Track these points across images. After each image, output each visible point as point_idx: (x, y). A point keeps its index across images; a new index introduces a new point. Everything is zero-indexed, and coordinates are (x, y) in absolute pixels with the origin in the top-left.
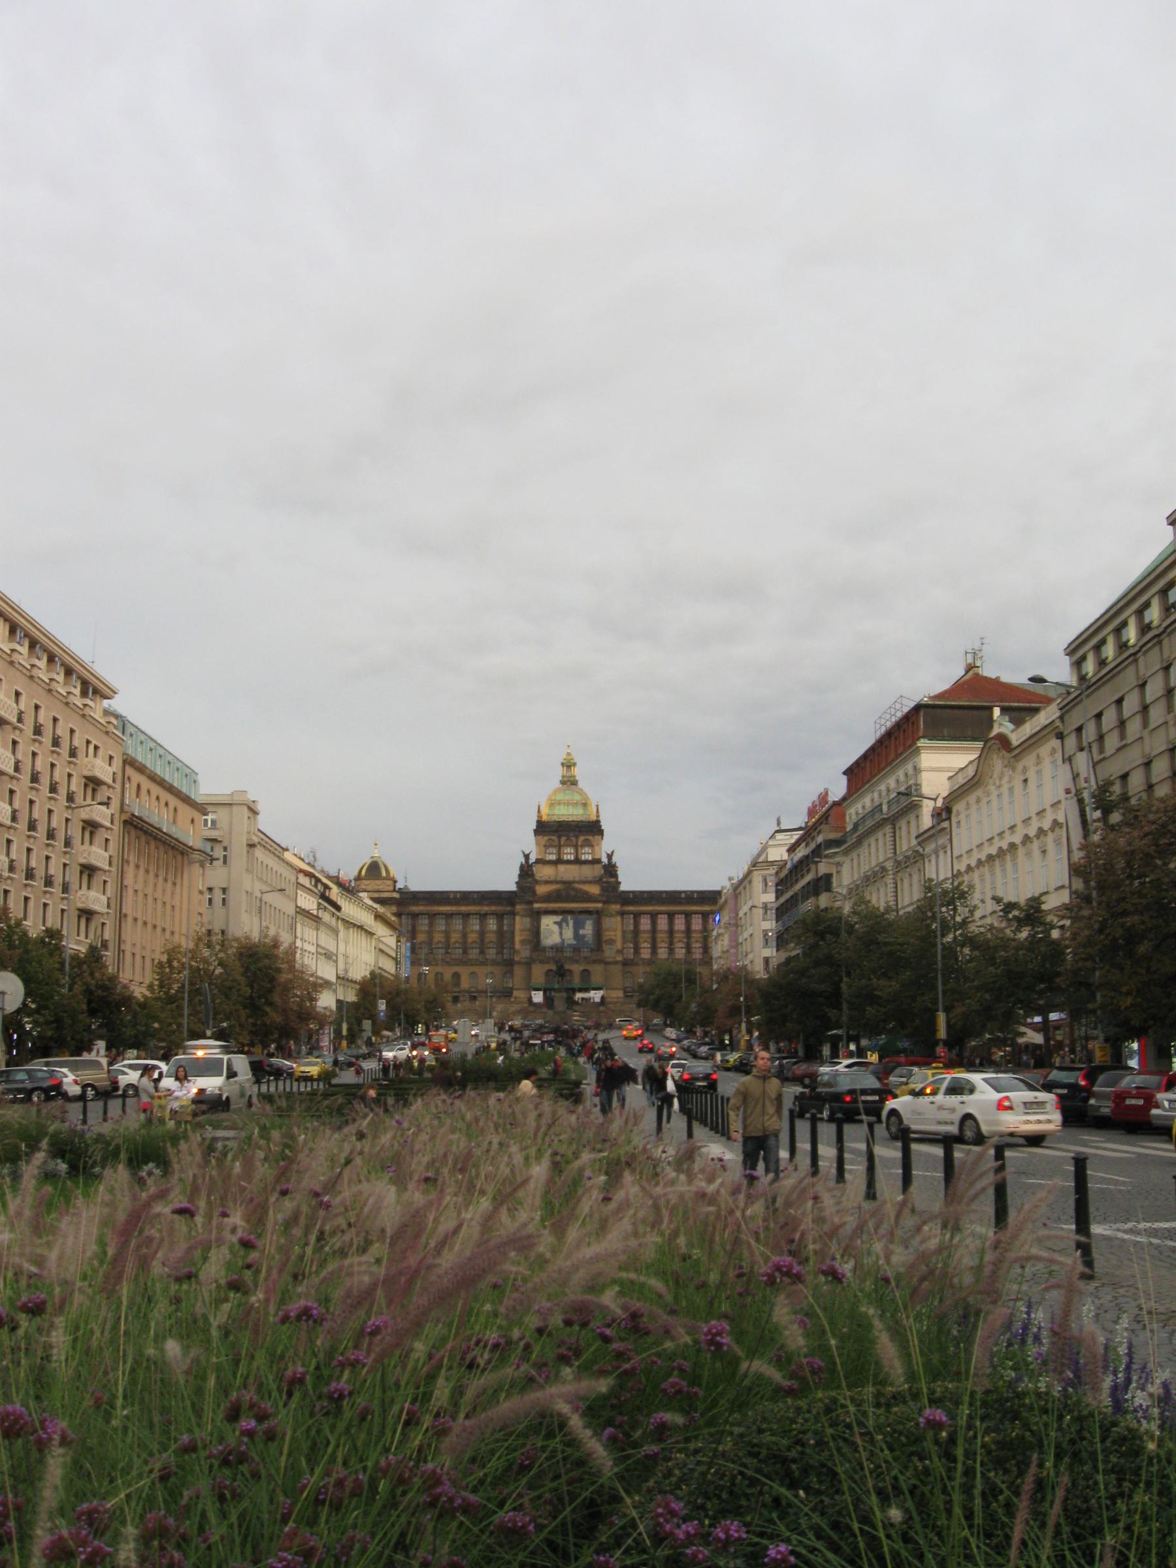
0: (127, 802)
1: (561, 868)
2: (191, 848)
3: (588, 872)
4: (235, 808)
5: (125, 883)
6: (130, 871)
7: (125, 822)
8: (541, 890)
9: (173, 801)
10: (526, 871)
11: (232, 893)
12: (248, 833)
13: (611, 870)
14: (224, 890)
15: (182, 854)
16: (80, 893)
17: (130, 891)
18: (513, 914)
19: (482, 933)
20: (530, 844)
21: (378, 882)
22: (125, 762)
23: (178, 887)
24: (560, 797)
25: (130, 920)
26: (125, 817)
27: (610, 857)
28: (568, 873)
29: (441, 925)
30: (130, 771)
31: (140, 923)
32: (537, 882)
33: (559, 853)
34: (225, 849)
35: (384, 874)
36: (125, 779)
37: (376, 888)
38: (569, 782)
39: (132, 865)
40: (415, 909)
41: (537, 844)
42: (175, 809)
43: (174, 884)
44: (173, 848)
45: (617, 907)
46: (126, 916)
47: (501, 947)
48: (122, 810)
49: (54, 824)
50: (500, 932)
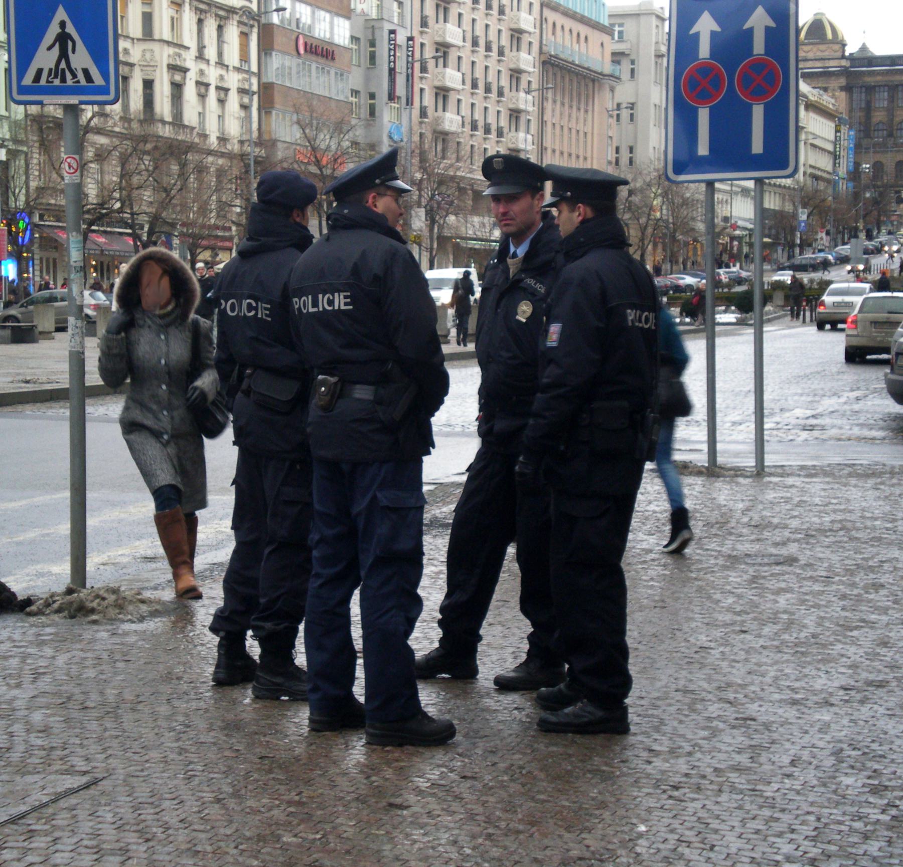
0: (544, 42)
2: (601, 74)
4: (643, 19)
5: (545, 119)
6: (549, 106)
7: (544, 63)
9: (584, 30)
11: (639, 108)
12: (657, 43)
14: (632, 106)
15: (593, 81)
16: (510, 135)
17: (549, 125)
21: (822, 47)
22: (542, 5)
23: (590, 113)
25: (549, 151)
26: (543, 59)
30: (547, 13)
31: (557, 153)
34: (633, 62)
35: (830, 35)
36: (543, 20)
37: (819, 54)
39: (550, 101)
42: (586, 38)
43: (586, 111)
44: (585, 77)
46: (546, 149)
48: (541, 52)
49: (490, 79)
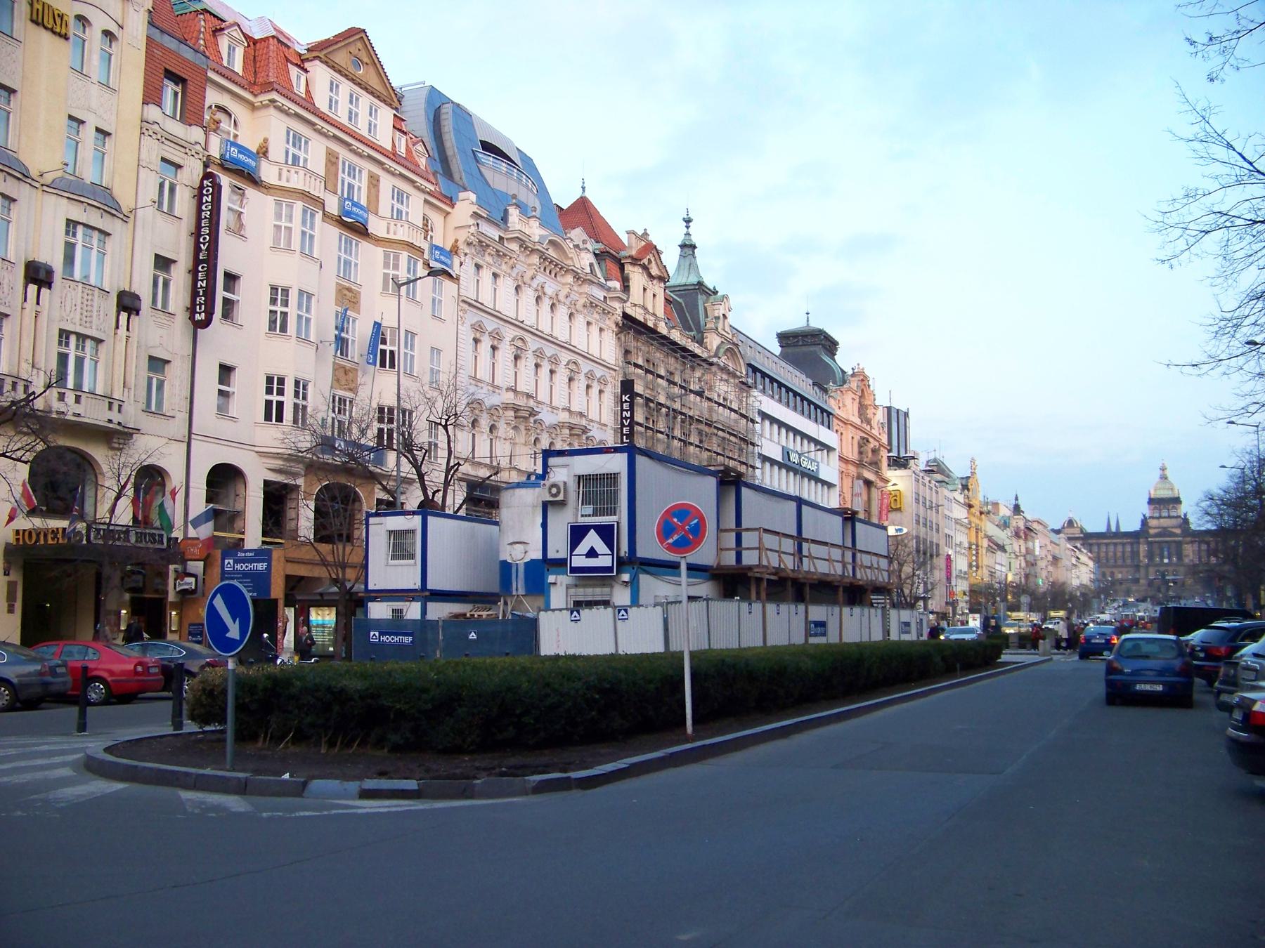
1: (1162, 520)
3: (1174, 522)
8: (1152, 531)
10: (1144, 522)
13: (1186, 521)
18: (1139, 543)
19: (1123, 552)
20: (1146, 510)
24: (1160, 486)
27: (1185, 515)
28: (1165, 523)
29: (1103, 549)
32: (1151, 528)
33: (1160, 513)
38: (1164, 478)
40: (1090, 541)
41: (1150, 509)
45: (1189, 539)
47: (1132, 558)
50: (1132, 552)
